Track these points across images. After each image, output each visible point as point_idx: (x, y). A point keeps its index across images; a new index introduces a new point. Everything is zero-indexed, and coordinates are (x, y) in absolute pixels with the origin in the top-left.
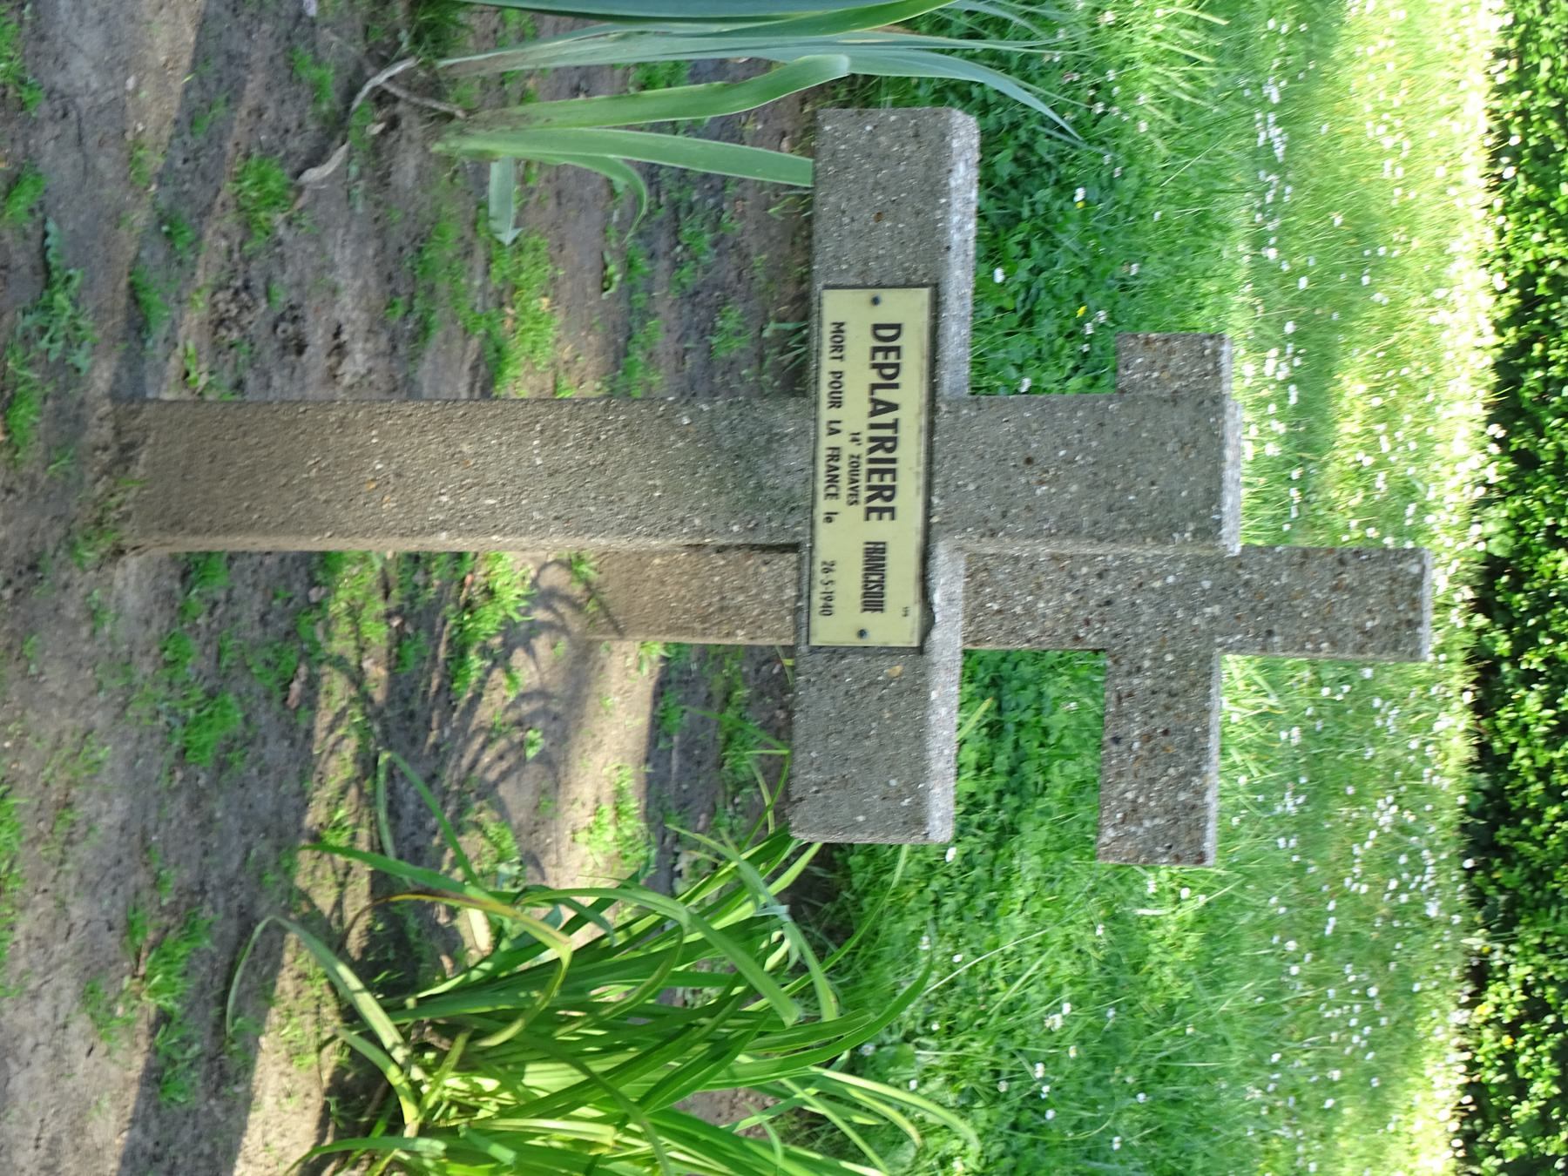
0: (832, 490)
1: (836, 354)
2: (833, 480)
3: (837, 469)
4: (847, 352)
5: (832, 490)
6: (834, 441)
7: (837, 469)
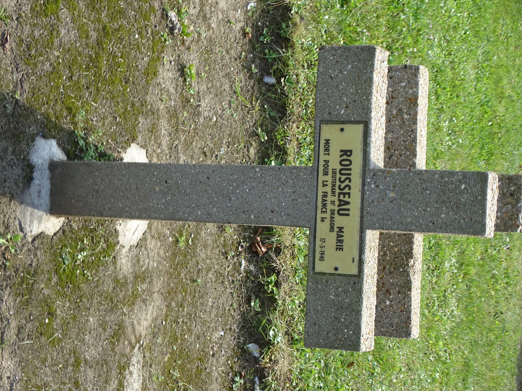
0: (324, 210)
1: (327, 153)
2: (324, 205)
3: (326, 201)
4: (330, 152)
5: (324, 210)
6: (325, 189)
7: (326, 201)
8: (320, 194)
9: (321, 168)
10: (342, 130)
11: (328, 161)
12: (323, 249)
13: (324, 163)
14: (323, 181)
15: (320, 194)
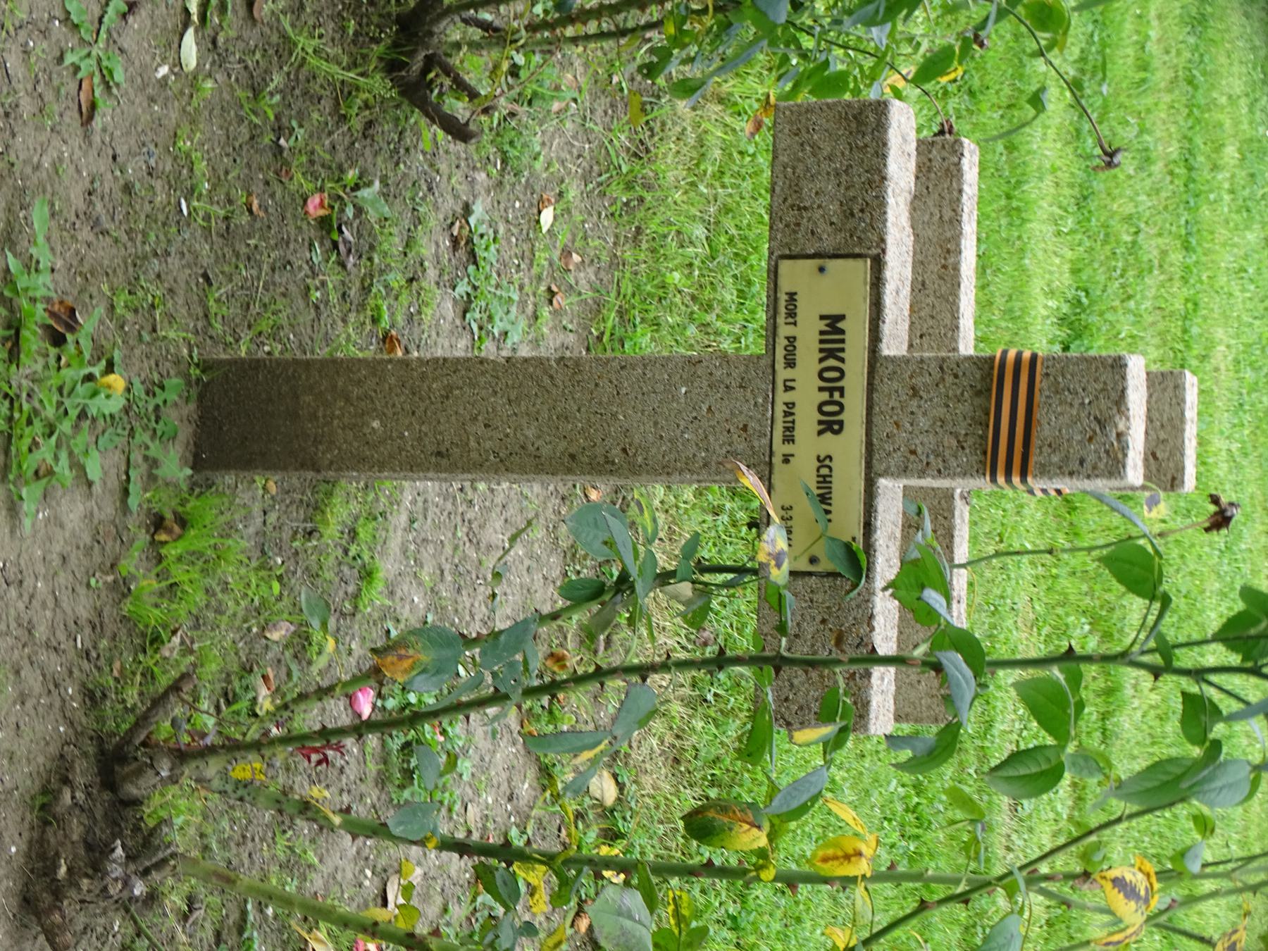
1: (790, 320)
4: (798, 319)
6: (788, 397)
8: (780, 408)
9: (780, 353)
10: (822, 270)
11: (795, 338)
12: (789, 523)
13: (786, 342)
14: (785, 381)
15: (780, 408)
